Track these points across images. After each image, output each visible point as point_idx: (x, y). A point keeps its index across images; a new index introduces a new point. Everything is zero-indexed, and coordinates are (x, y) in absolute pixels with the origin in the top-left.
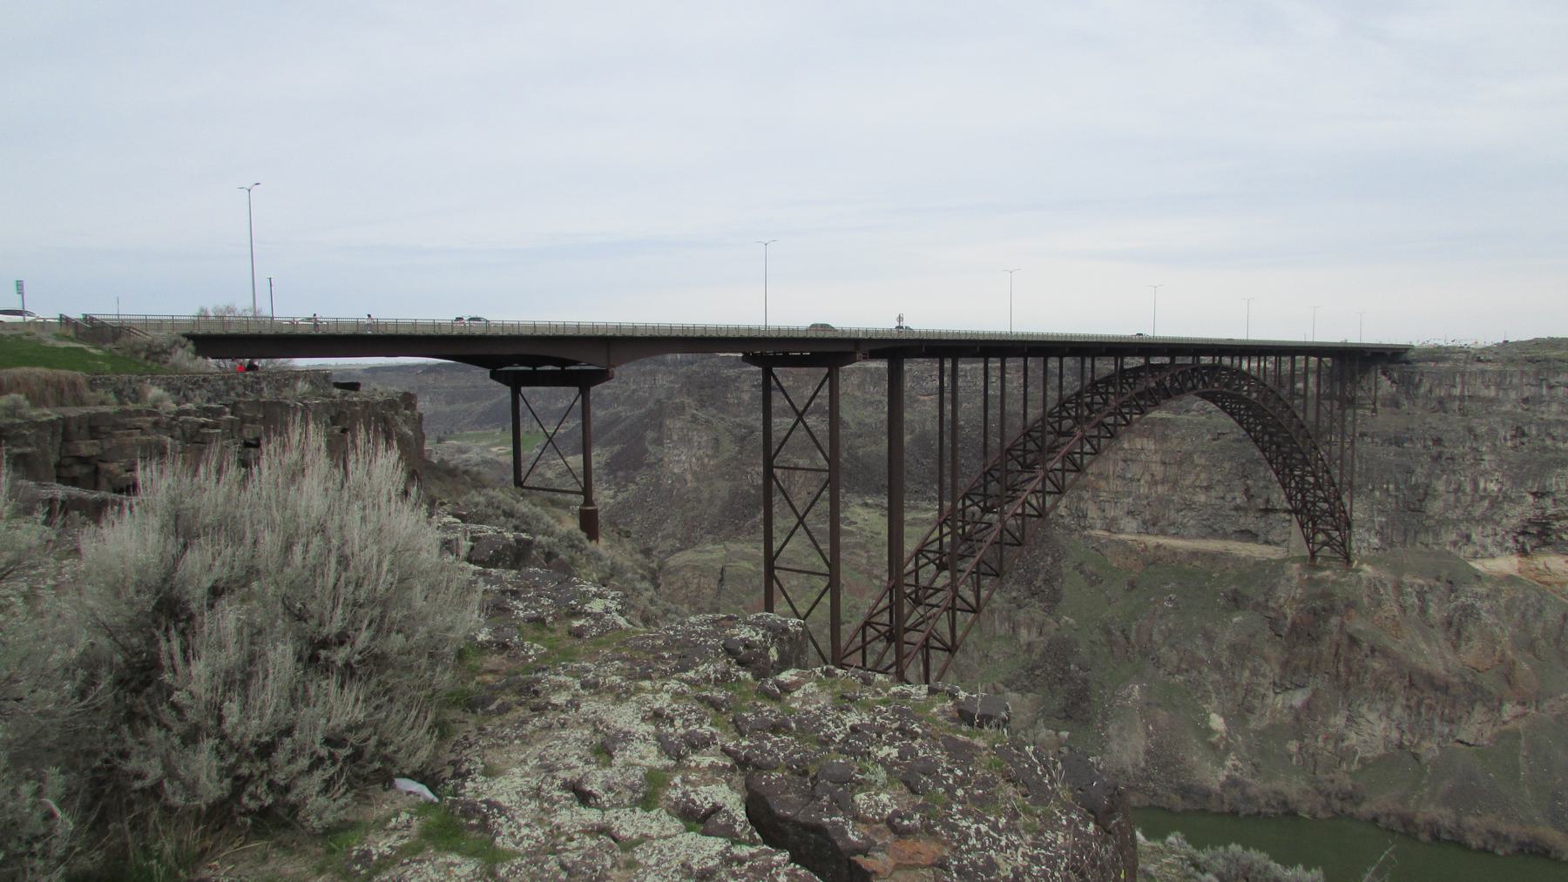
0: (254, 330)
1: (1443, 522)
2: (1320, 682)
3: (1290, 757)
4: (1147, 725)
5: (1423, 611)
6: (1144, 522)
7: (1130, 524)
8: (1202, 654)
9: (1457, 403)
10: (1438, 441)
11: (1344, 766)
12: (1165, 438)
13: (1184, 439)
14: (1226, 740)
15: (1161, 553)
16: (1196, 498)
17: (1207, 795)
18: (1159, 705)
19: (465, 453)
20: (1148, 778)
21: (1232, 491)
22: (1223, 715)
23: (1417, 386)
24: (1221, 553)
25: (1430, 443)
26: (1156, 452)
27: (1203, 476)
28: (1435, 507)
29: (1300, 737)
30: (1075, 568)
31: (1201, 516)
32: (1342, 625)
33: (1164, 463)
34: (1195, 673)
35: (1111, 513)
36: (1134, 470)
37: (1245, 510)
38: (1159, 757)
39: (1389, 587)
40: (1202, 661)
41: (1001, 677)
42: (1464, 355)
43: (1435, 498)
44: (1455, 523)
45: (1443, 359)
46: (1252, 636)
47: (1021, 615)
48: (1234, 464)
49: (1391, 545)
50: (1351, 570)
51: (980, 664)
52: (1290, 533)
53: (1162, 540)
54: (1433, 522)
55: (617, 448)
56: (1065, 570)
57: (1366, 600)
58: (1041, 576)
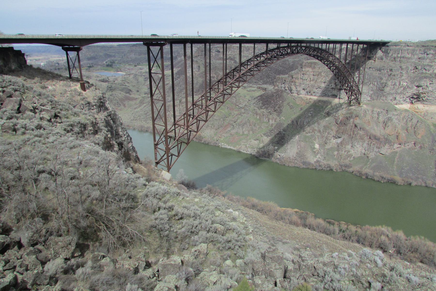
1: (388, 94)
2: (345, 137)
3: (334, 156)
4: (298, 146)
5: (378, 118)
6: (307, 92)
7: (303, 92)
8: (316, 128)
9: (399, 59)
10: (391, 70)
11: (349, 159)
12: (314, 68)
13: (319, 68)
14: (318, 151)
15: (311, 100)
16: (321, 85)
17: (309, 164)
18: (302, 141)
19: (142, 69)
20: (296, 159)
21: (331, 83)
22: (319, 145)
23: (388, 54)
24: (327, 101)
25: (389, 71)
26: (312, 72)
28: (387, 89)
29: (338, 151)
30: (287, 104)
32: (354, 121)
33: (313, 75)
34: (313, 133)
35: (298, 89)
36: (306, 77)
37: (335, 89)
38: (299, 154)
39: (370, 112)
40: (315, 130)
41: (263, 133)
42: (405, 44)
43: (387, 87)
44: (392, 94)
45: (398, 45)
46: (330, 124)
47: (271, 117)
49: (373, 100)
50: (360, 107)
51: (258, 129)
53: (312, 97)
54: (386, 94)
55: (179, 69)
56: (284, 105)
57: (362, 115)
58: (278, 106)
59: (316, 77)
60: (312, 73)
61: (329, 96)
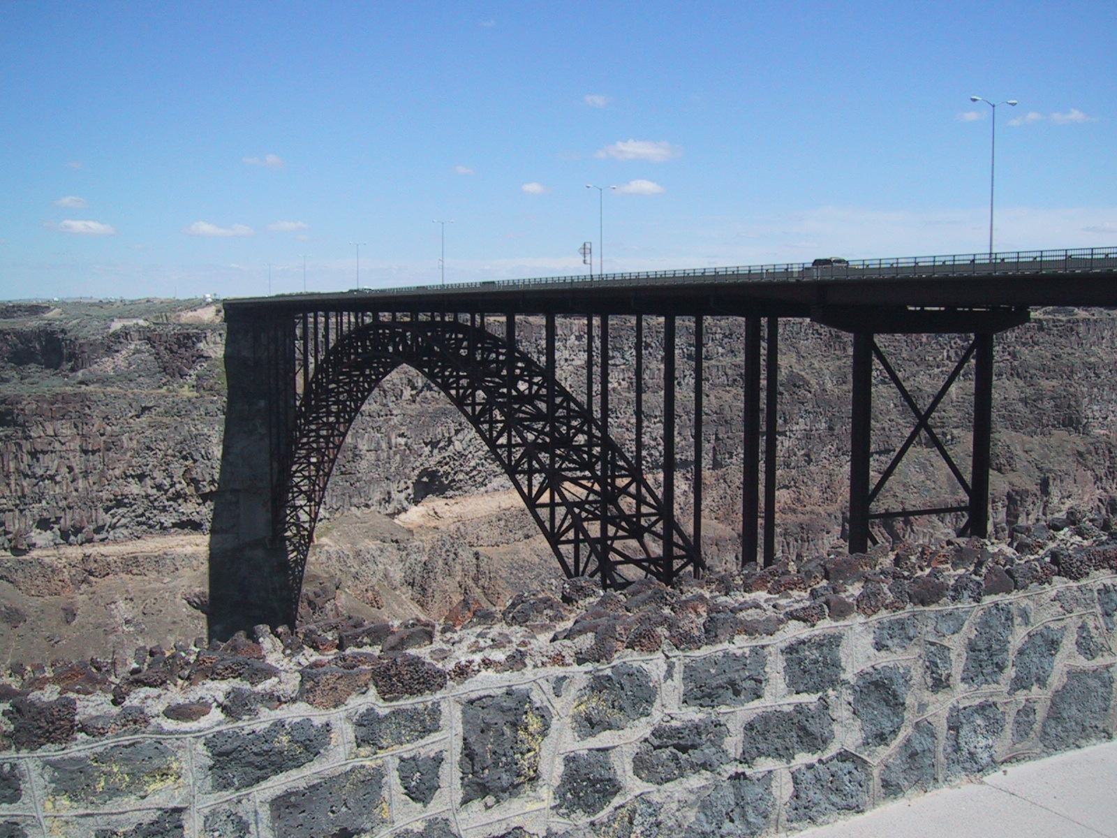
7: (41, 538)
16: (126, 490)
26: (73, 439)
31: (134, 511)
33: (85, 452)
36: (49, 463)
44: (378, 481)
53: (89, 549)
59: (95, 459)
60: (76, 444)
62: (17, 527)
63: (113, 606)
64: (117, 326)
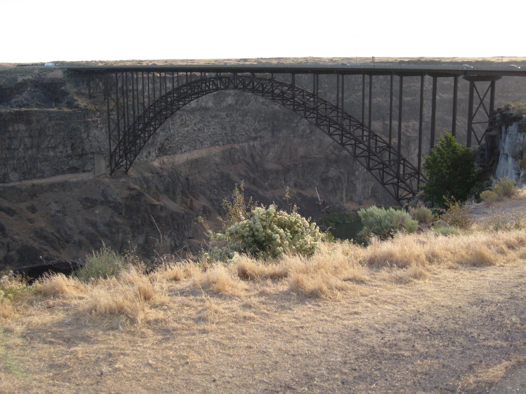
0: (372, 66)
7: (14, 176)
27: (52, 141)
48: (66, 133)
52: (94, 164)
53: (35, 181)
60: (26, 134)
61: (63, 173)
62: (3, 172)
63: (50, 205)
64: (20, 79)
